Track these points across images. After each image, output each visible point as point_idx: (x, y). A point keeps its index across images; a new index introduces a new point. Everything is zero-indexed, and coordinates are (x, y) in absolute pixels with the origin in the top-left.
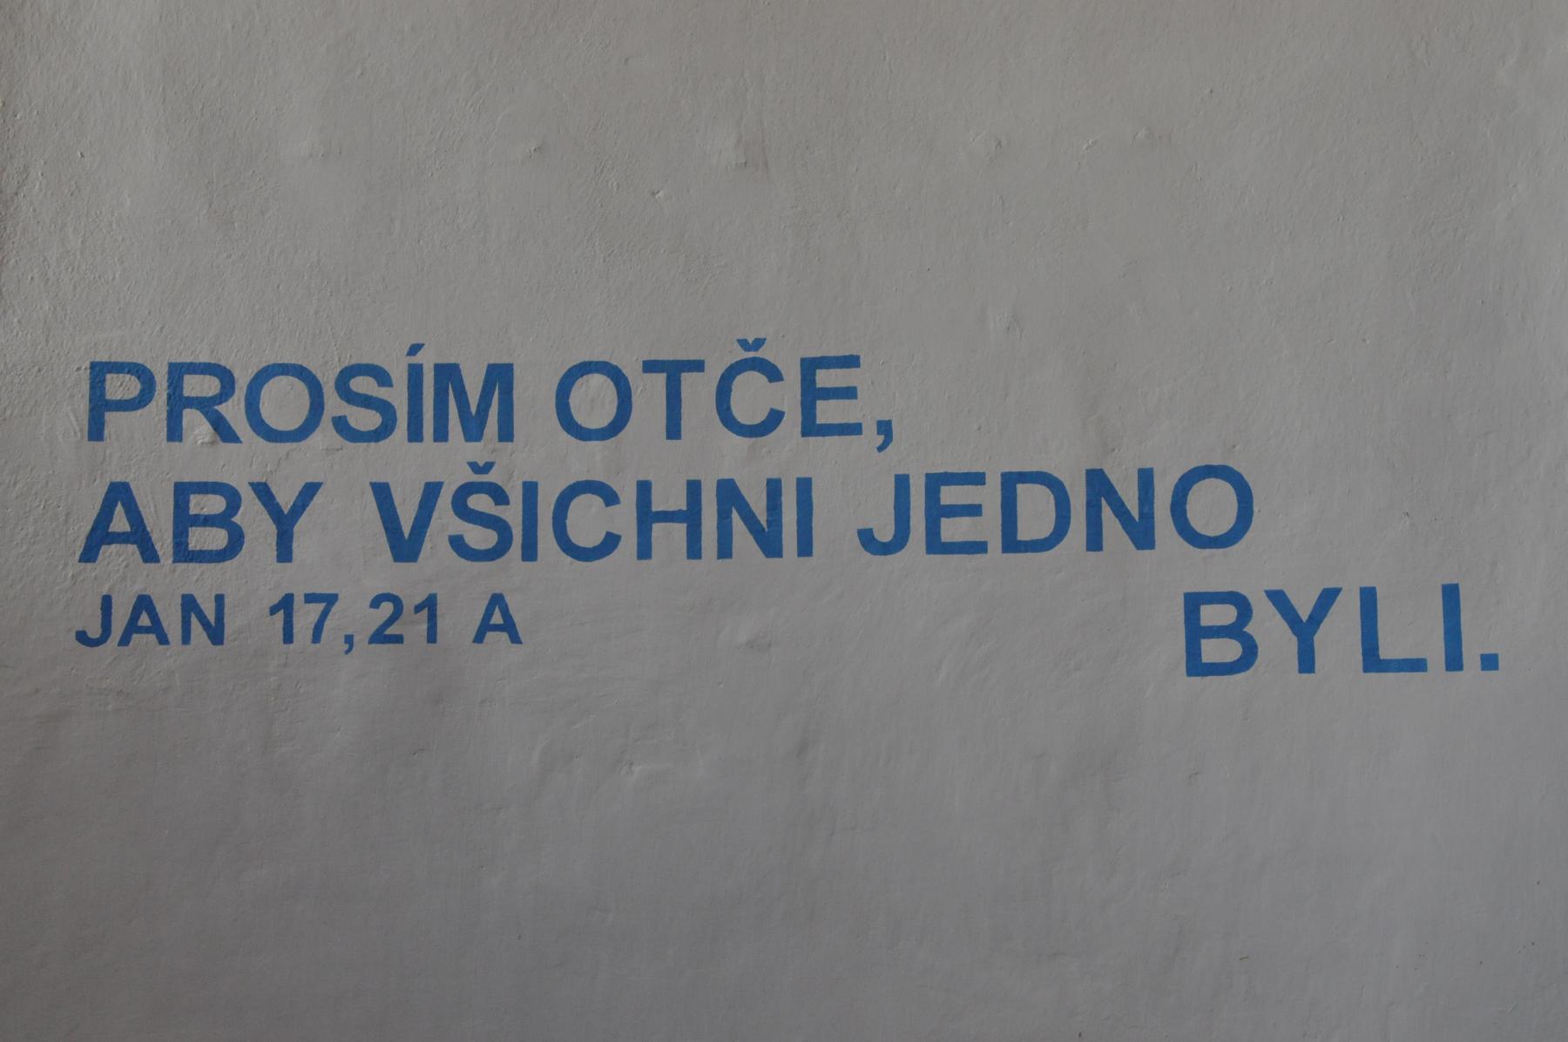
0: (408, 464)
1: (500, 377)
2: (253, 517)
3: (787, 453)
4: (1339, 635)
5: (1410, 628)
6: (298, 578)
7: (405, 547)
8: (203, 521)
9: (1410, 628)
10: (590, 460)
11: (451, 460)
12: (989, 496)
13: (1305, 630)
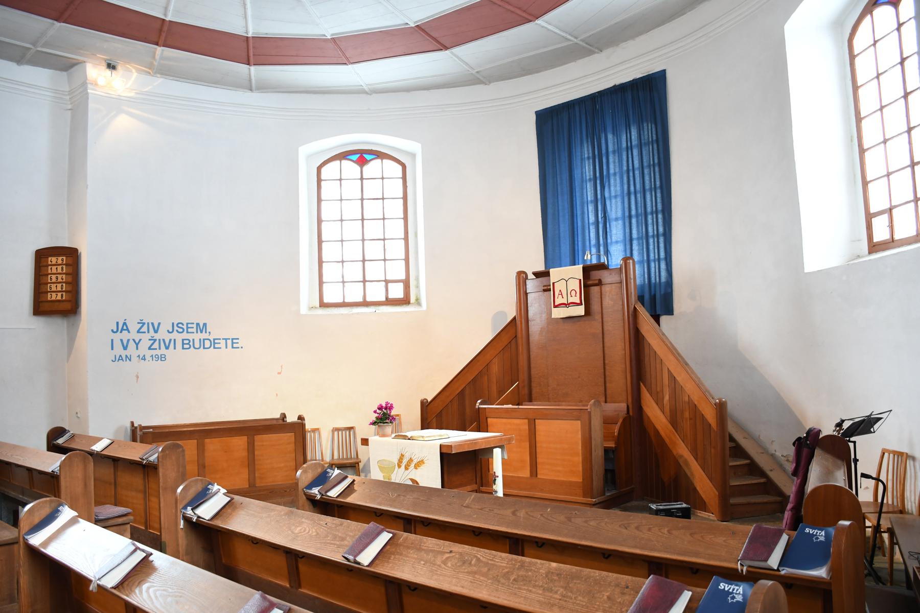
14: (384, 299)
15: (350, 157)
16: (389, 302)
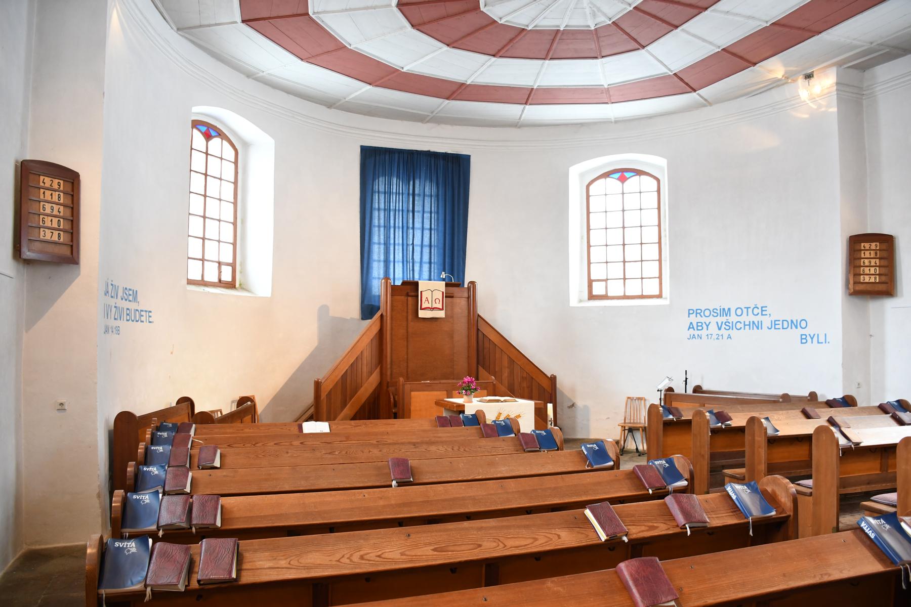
0: (721, 319)
1: (729, 309)
2: (704, 326)
3: (759, 318)
4: (815, 339)
6: (709, 332)
7: (720, 329)
8: (700, 326)
9: (822, 339)
10: (739, 319)
11: (724, 319)
12: (780, 323)
14: (216, 280)
15: (200, 127)
16: (221, 284)
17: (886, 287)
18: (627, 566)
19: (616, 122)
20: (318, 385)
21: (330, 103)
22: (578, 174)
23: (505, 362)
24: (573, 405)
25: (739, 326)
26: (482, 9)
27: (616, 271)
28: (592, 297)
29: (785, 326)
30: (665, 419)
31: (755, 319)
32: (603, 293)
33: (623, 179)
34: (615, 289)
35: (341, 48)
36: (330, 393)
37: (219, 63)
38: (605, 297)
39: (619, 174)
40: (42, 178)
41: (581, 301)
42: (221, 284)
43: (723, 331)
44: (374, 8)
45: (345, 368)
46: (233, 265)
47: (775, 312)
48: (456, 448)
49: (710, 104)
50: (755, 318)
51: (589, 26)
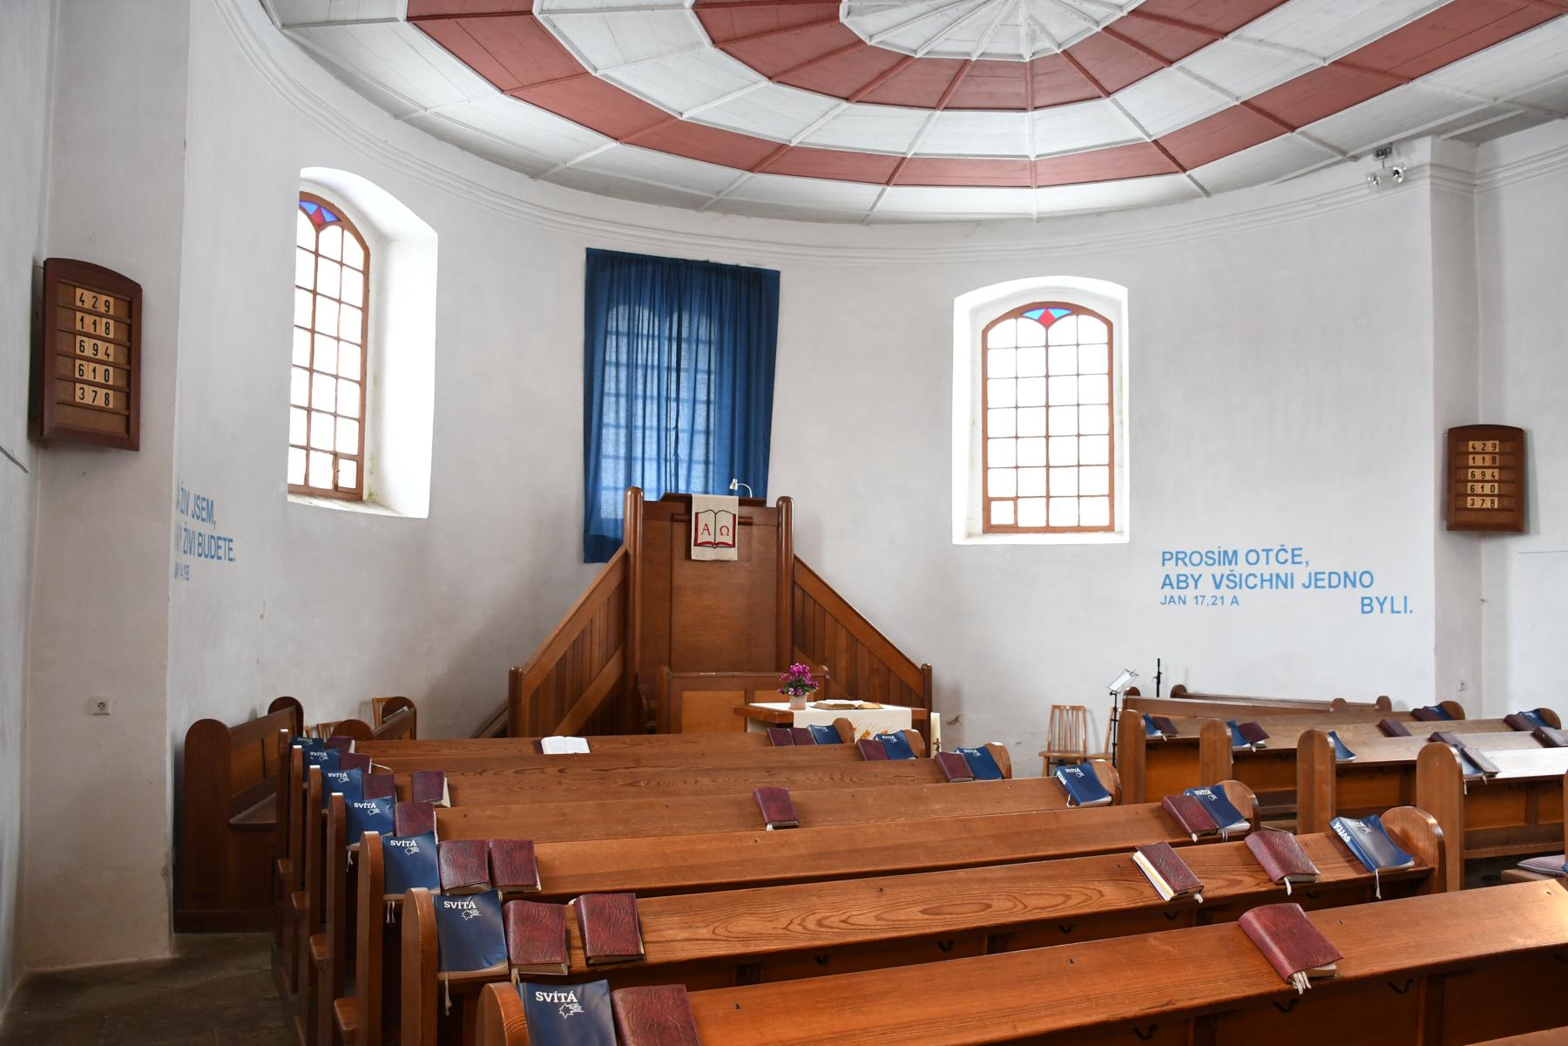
0: (1218, 570)
1: (1235, 552)
2: (1190, 581)
4: (1387, 606)
5: (1399, 606)
6: (1198, 592)
7: (1218, 587)
8: (1182, 582)
9: (1399, 606)
10: (1252, 569)
11: (1226, 569)
12: (1326, 577)
13: (1382, 605)
14: (329, 486)
16: (337, 492)
17: (1511, 517)
18: (1257, 917)
19: (1041, 219)
20: (515, 677)
21: (537, 169)
22: (968, 308)
23: (842, 641)
24: (957, 720)
25: (1251, 582)
26: (843, 18)
27: (1033, 482)
28: (989, 528)
29: (1335, 582)
30: (1149, 737)
31: (1282, 570)
32: (1011, 521)
33: (1047, 321)
34: (1031, 515)
35: (580, 73)
36: (535, 697)
37: (347, 89)
38: (1014, 529)
39: (1038, 314)
40: (79, 291)
41: (969, 535)
42: (337, 492)
43: (1223, 591)
44: (652, 8)
45: (562, 649)
46: (359, 459)
47: (1318, 560)
48: (837, 777)
49: (1207, 193)
50: (1280, 569)
51: (1021, 56)
